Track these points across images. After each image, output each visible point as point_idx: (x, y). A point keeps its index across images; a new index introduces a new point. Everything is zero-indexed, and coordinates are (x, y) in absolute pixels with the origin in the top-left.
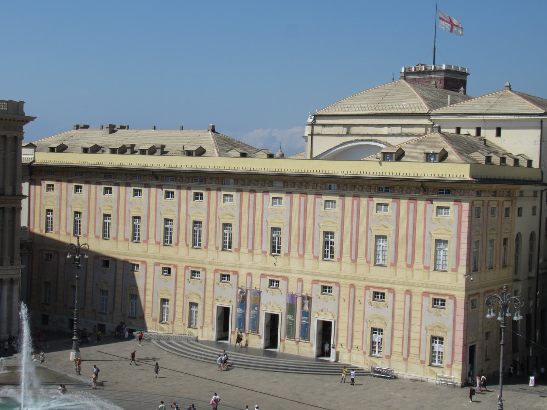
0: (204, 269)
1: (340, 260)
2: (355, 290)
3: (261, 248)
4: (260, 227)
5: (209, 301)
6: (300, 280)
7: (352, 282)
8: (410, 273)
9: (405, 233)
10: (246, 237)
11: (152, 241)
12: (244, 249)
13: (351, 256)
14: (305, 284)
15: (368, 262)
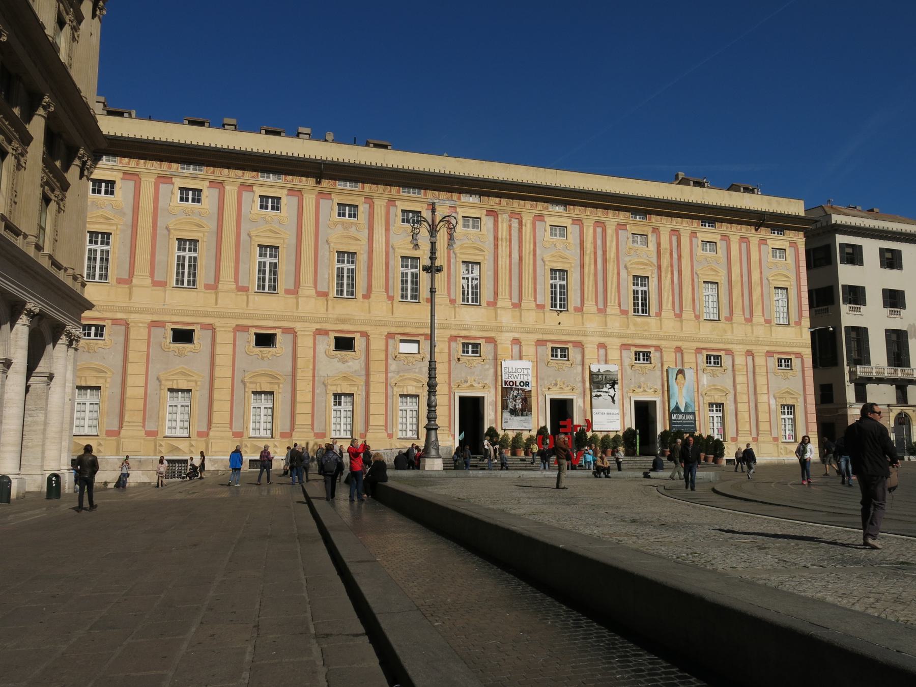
1: (659, 314)
3: (535, 300)
6: (602, 346)
7: (679, 344)
8: (748, 328)
9: (739, 278)
11: (307, 289)
12: (504, 302)
14: (609, 352)
15: (697, 317)
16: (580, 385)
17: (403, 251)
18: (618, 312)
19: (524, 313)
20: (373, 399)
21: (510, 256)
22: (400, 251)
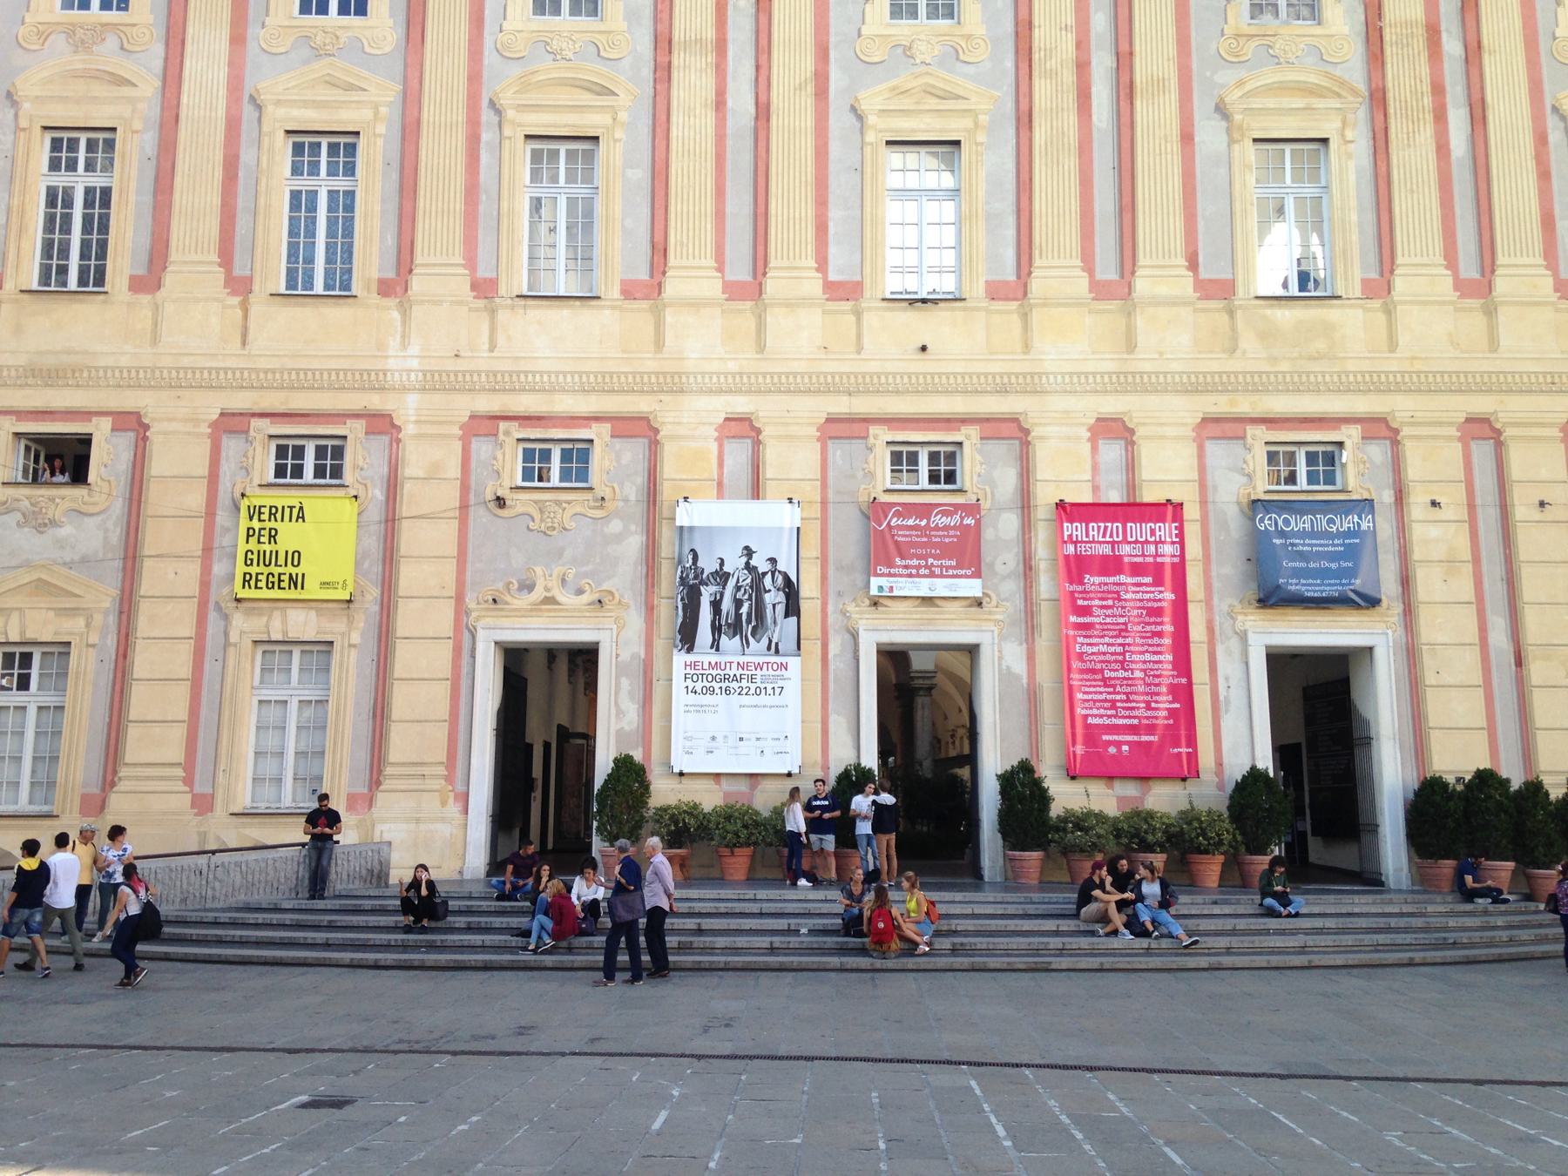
0: (381, 424)
2: (1499, 445)
3: (822, 264)
4: (806, 146)
5: (423, 621)
6: (1112, 429)
7: (1481, 405)
10: (709, 206)
12: (693, 277)
13: (1451, 260)
16: (1011, 587)
17: (295, 113)
18: (1184, 285)
19: (777, 320)
20: (144, 662)
21: (720, 104)
22: (281, 112)
